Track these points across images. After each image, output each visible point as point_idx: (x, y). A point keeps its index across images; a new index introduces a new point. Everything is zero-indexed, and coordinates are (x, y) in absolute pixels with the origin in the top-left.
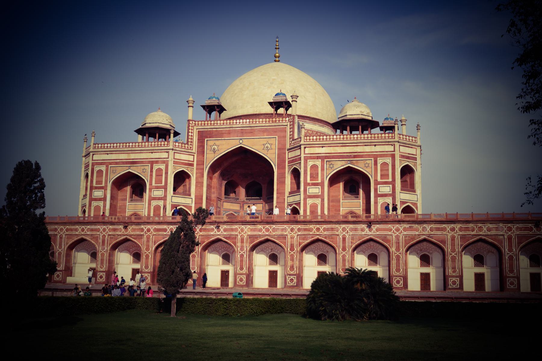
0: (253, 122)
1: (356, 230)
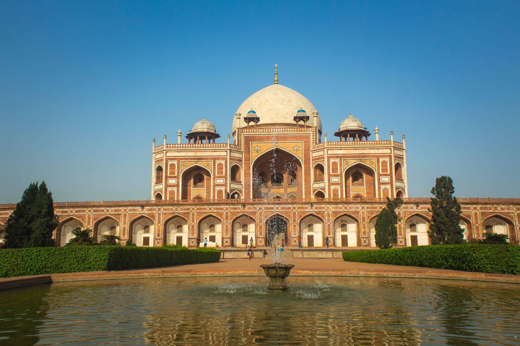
1: (407, 208)
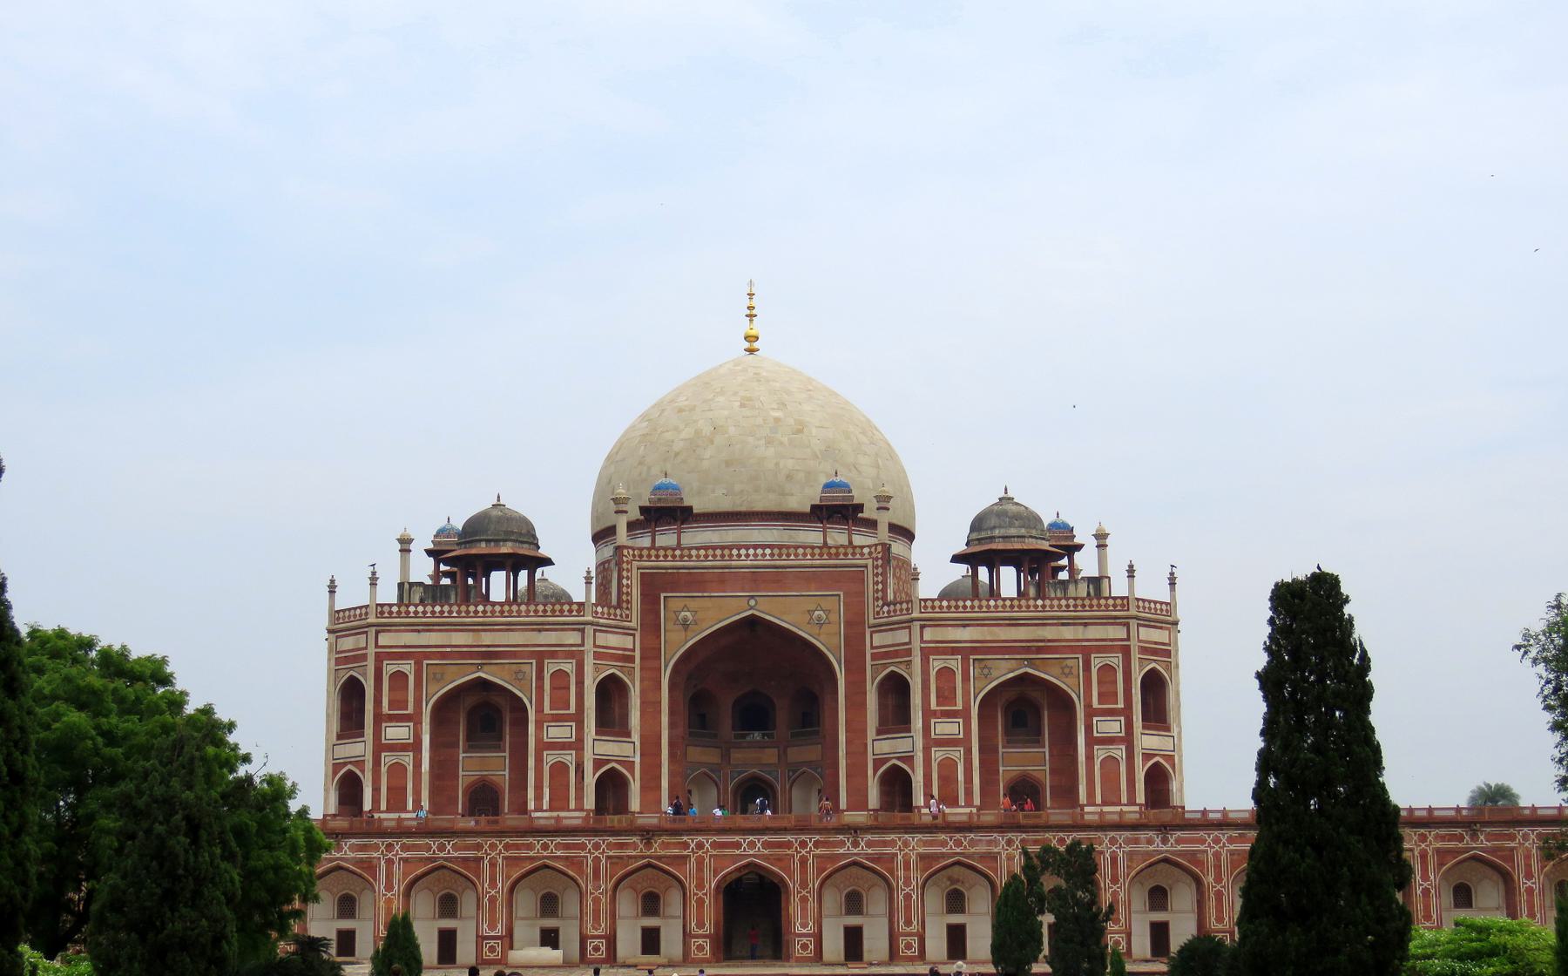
0: (780, 555)
1: (1136, 841)
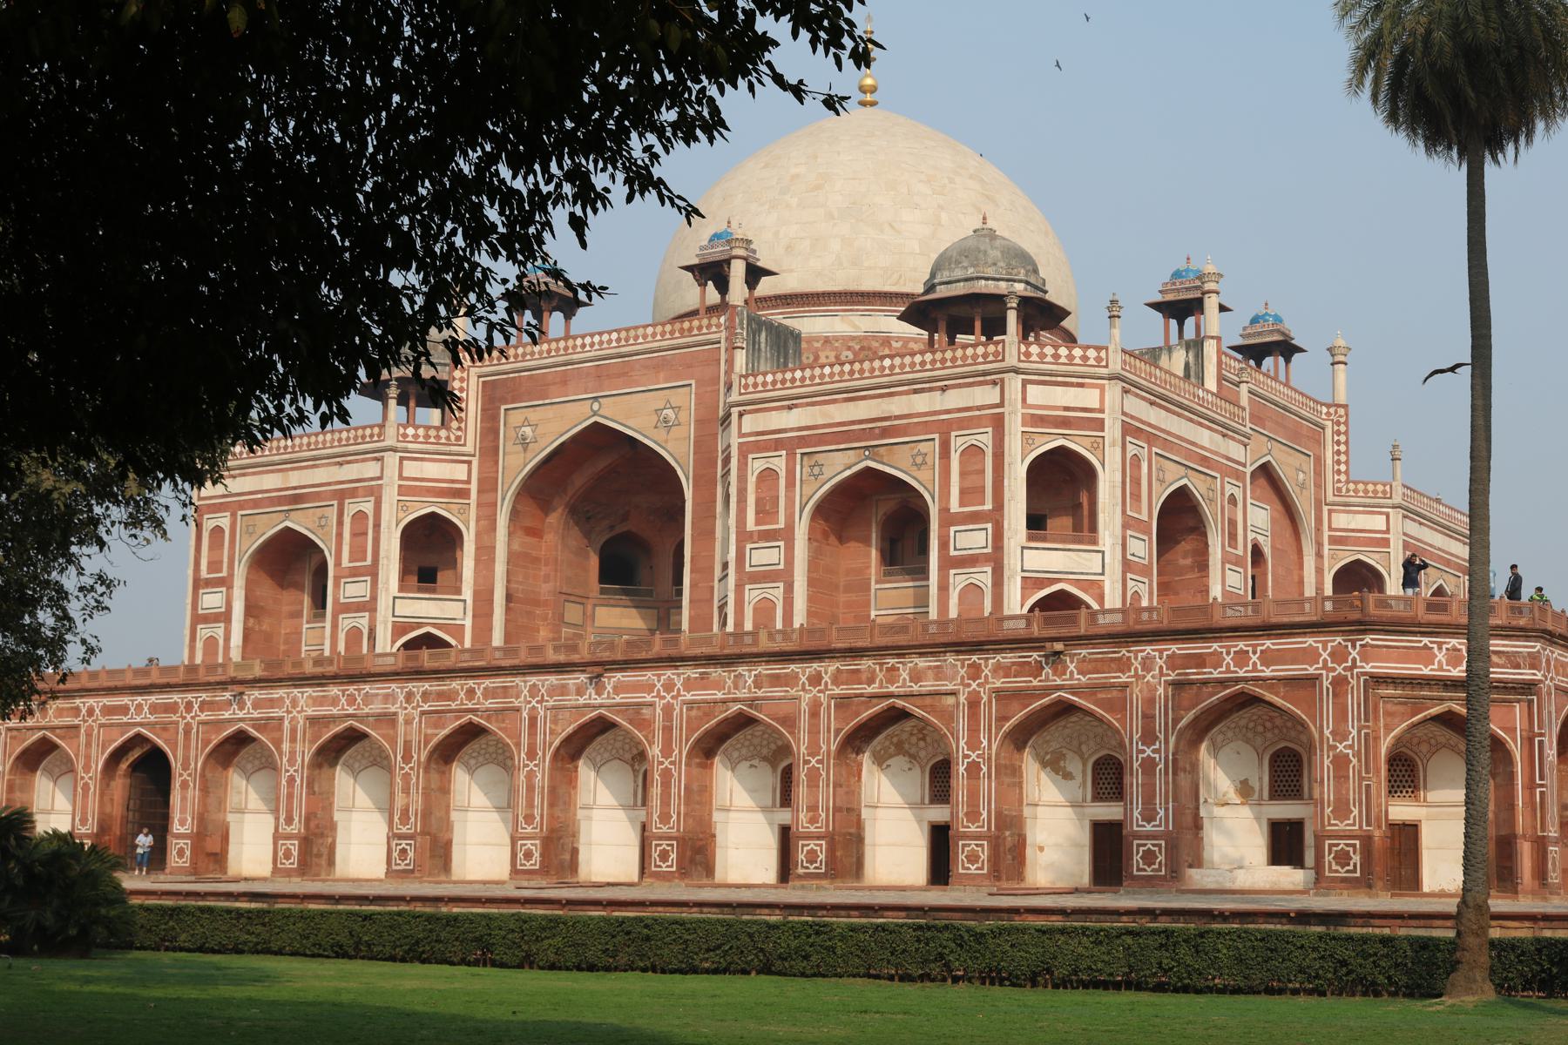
0: (627, 340)
1: (563, 690)
